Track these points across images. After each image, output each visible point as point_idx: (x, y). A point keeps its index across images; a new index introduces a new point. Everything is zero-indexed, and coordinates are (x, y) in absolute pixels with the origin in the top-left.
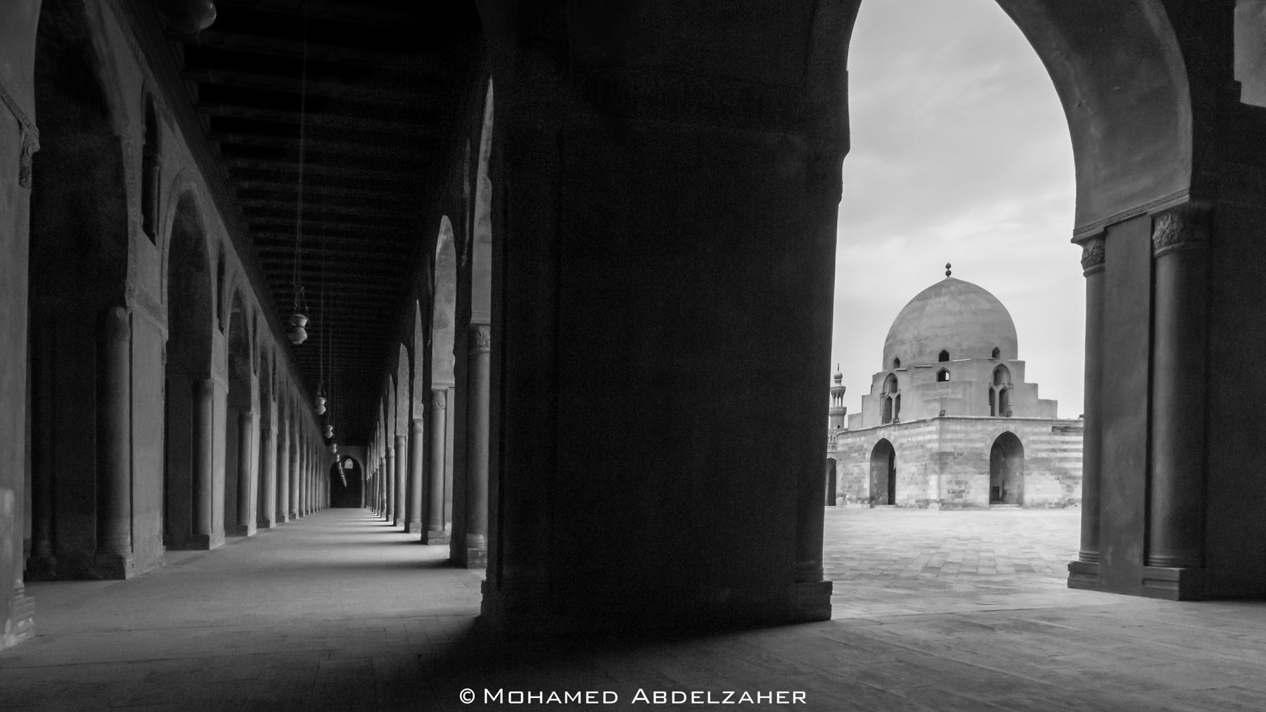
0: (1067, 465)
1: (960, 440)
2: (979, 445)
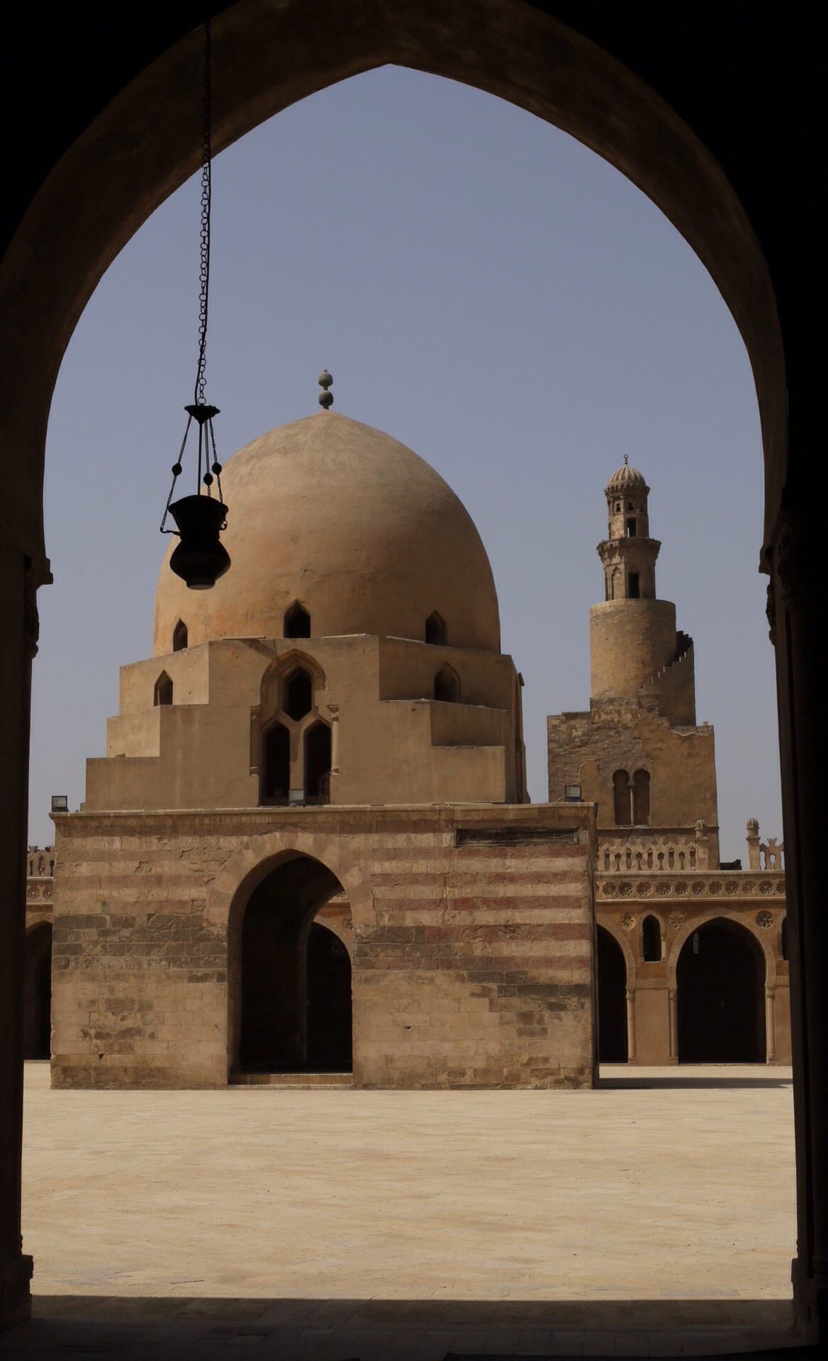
1: (123, 881)
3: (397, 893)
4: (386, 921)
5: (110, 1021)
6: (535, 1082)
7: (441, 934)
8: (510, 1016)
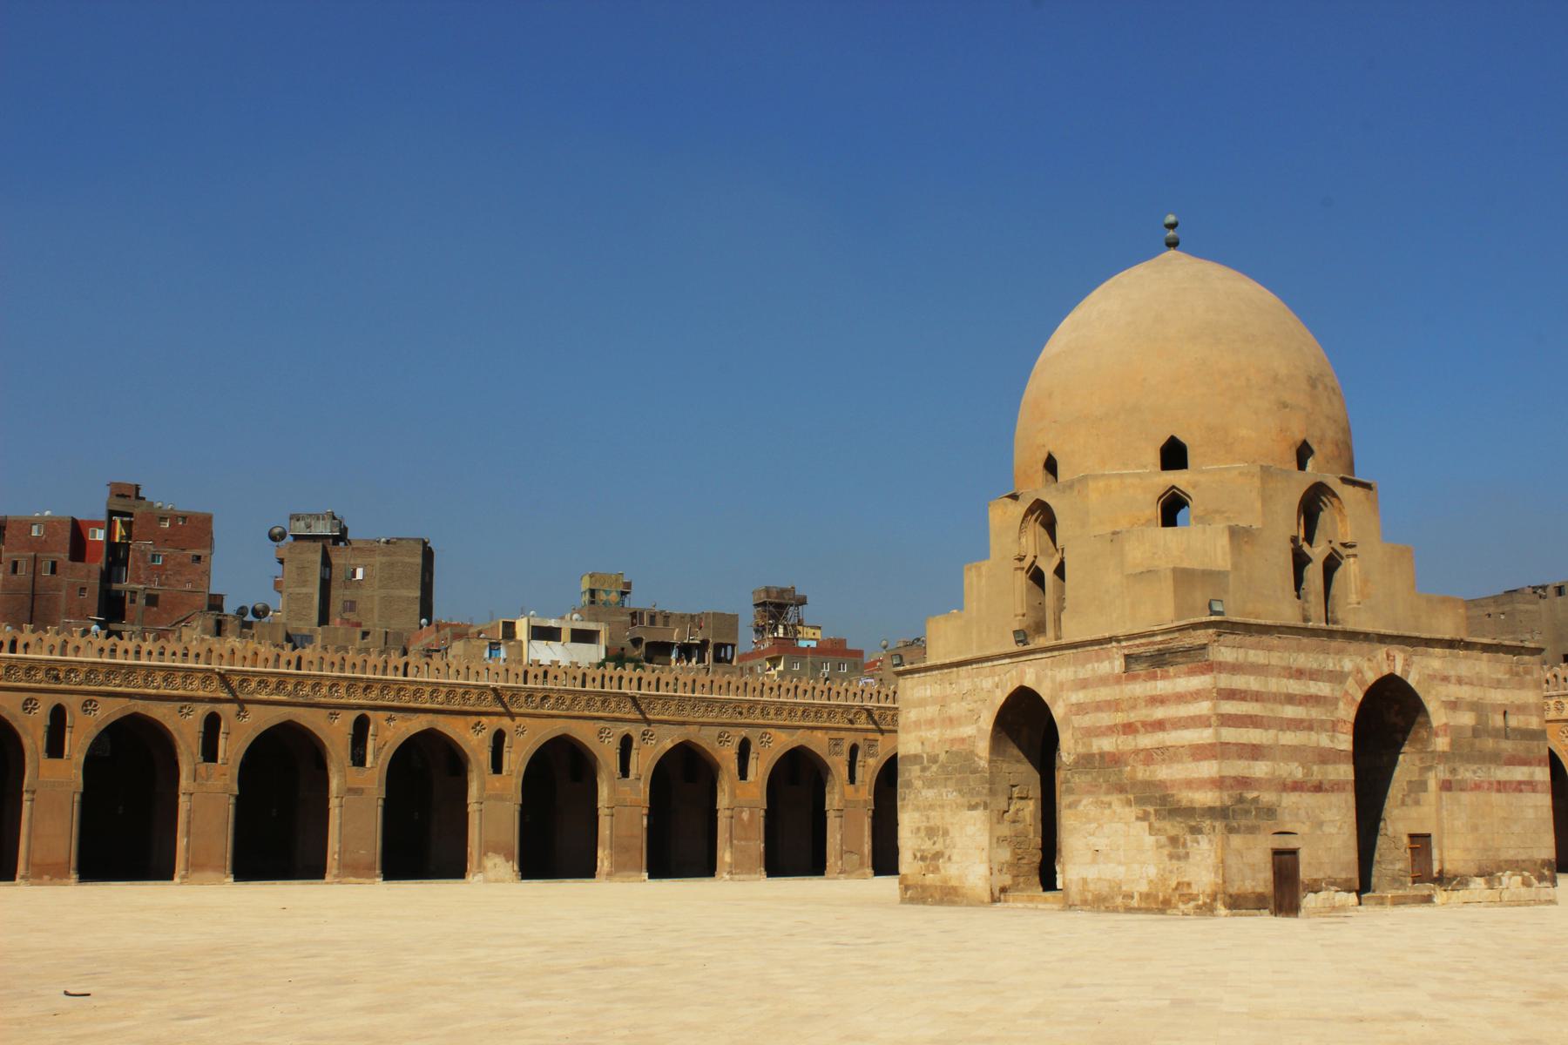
0: (1163, 773)
1: (931, 723)
2: (968, 730)
3: (1087, 721)
4: (1081, 750)
5: (927, 845)
6: (1181, 906)
7: (1113, 760)
8: (1163, 839)
